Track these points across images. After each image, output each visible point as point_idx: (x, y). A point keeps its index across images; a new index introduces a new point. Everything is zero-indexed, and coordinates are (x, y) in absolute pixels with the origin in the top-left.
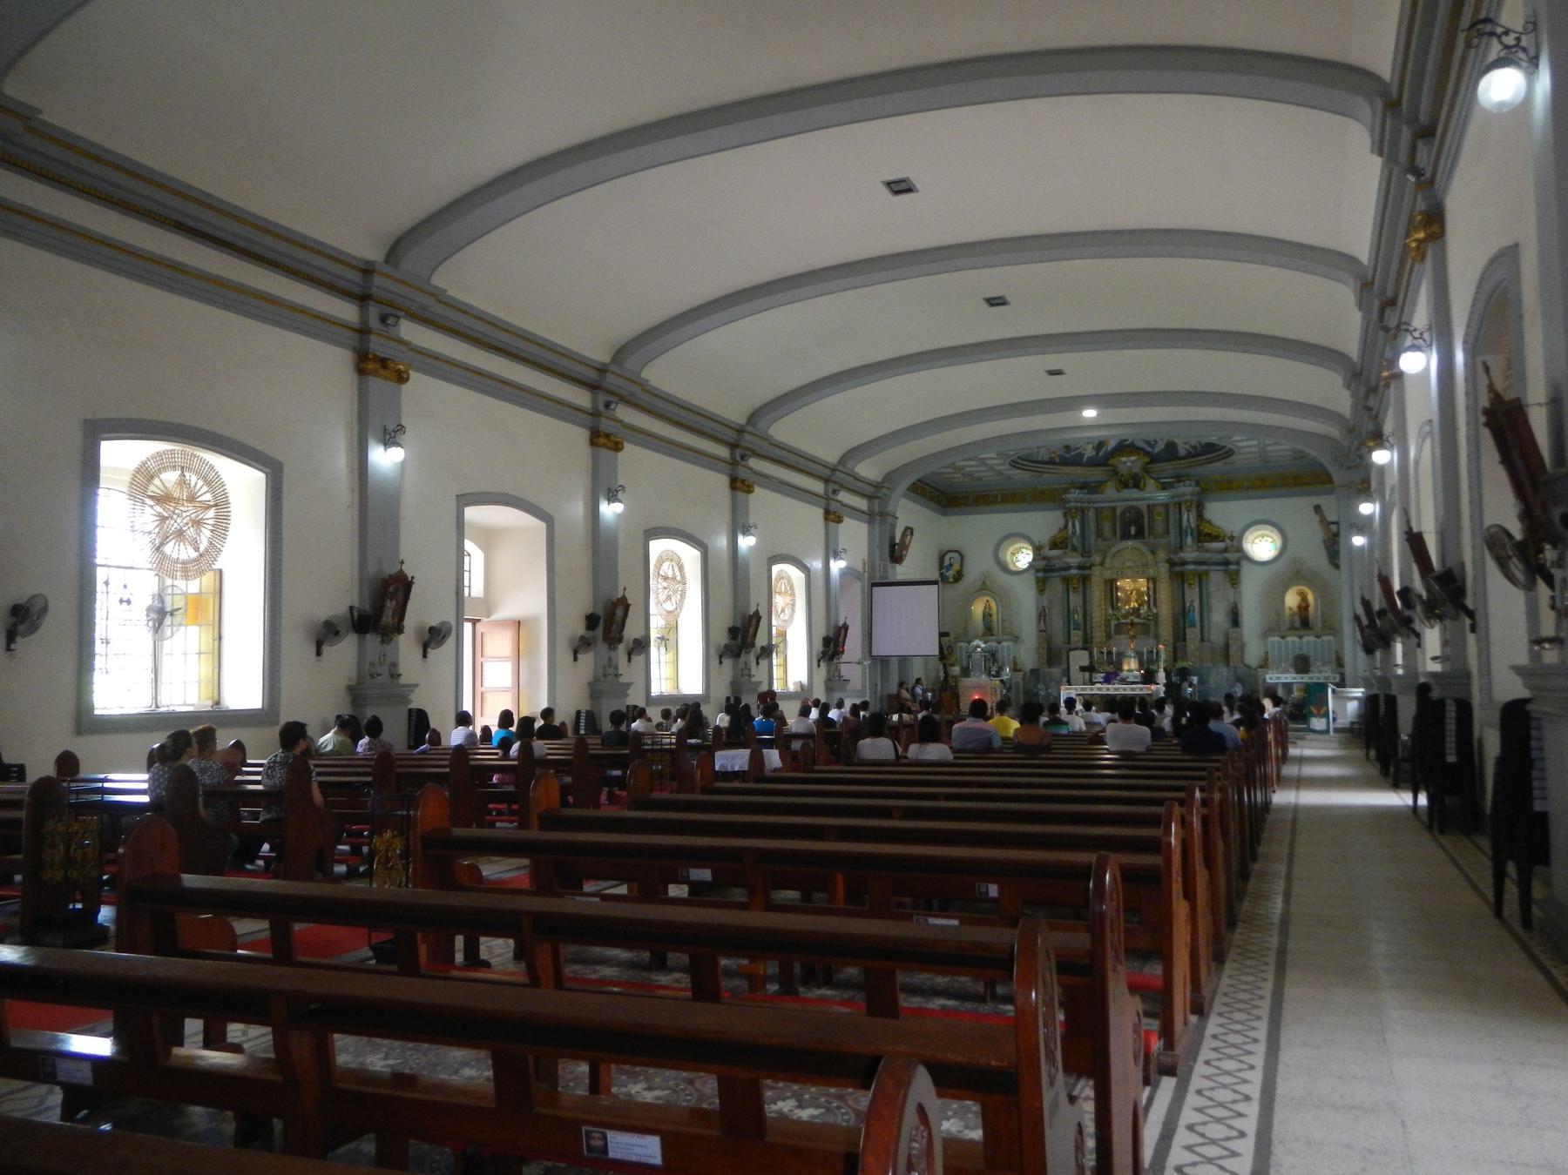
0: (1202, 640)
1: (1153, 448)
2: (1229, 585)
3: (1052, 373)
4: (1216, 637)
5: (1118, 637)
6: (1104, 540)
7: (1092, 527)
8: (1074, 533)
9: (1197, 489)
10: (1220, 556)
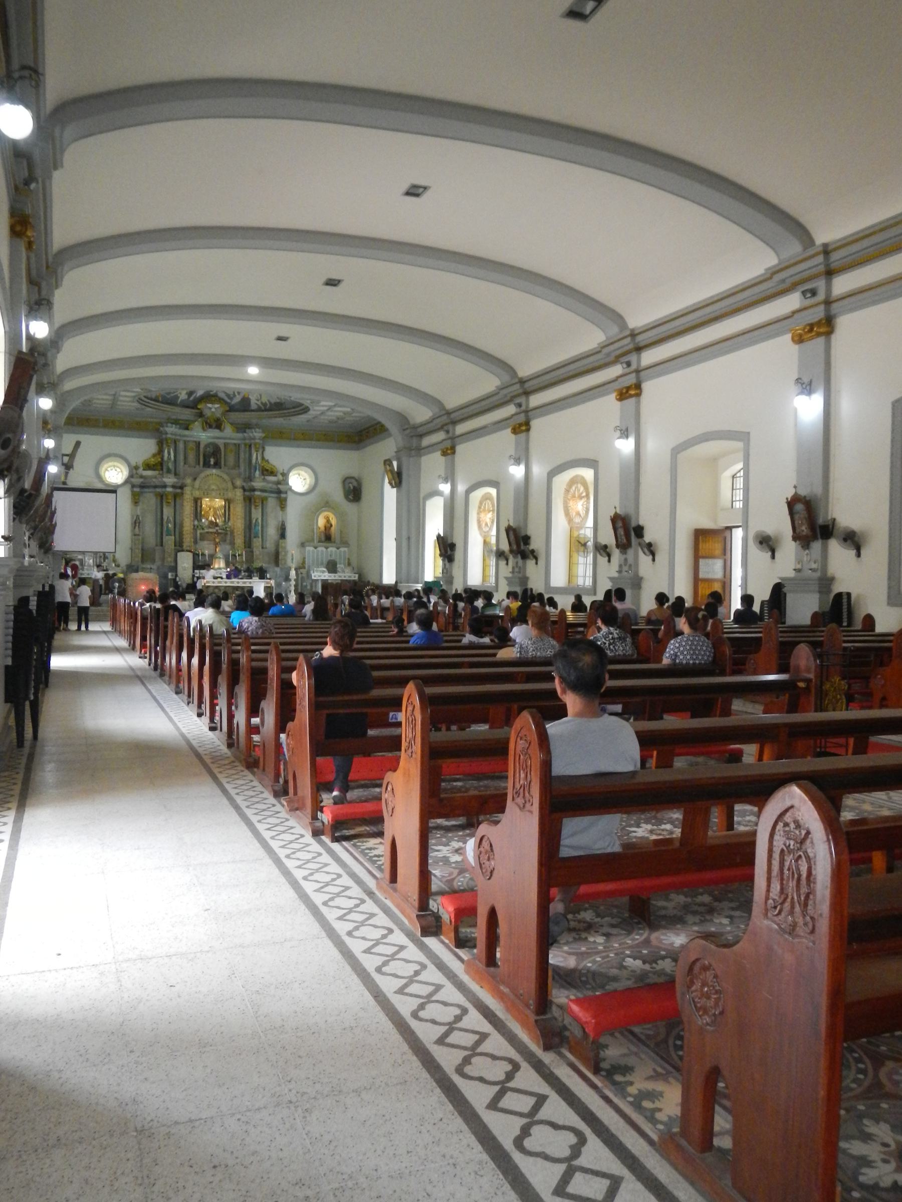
0: (262, 548)
2: (279, 508)
3: (280, 339)
4: (270, 545)
6: (189, 466)
8: (169, 458)
9: (264, 435)
10: (275, 486)
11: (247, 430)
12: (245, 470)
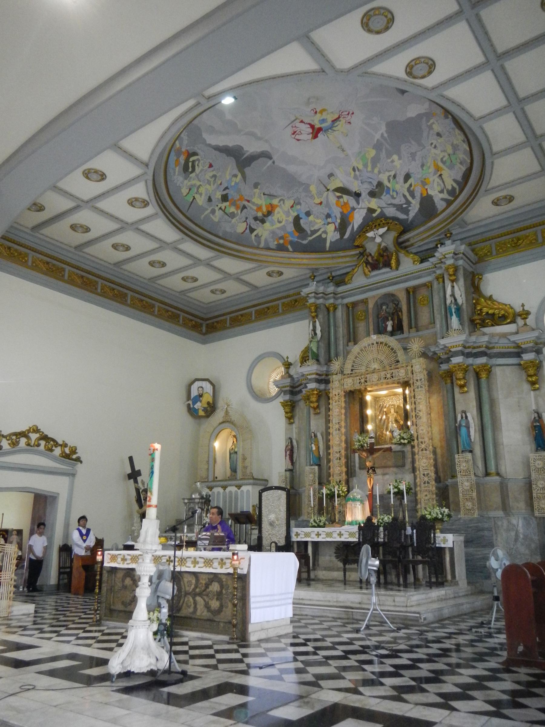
1: (408, 215)
2: (526, 386)
5: (362, 471)
7: (341, 331)
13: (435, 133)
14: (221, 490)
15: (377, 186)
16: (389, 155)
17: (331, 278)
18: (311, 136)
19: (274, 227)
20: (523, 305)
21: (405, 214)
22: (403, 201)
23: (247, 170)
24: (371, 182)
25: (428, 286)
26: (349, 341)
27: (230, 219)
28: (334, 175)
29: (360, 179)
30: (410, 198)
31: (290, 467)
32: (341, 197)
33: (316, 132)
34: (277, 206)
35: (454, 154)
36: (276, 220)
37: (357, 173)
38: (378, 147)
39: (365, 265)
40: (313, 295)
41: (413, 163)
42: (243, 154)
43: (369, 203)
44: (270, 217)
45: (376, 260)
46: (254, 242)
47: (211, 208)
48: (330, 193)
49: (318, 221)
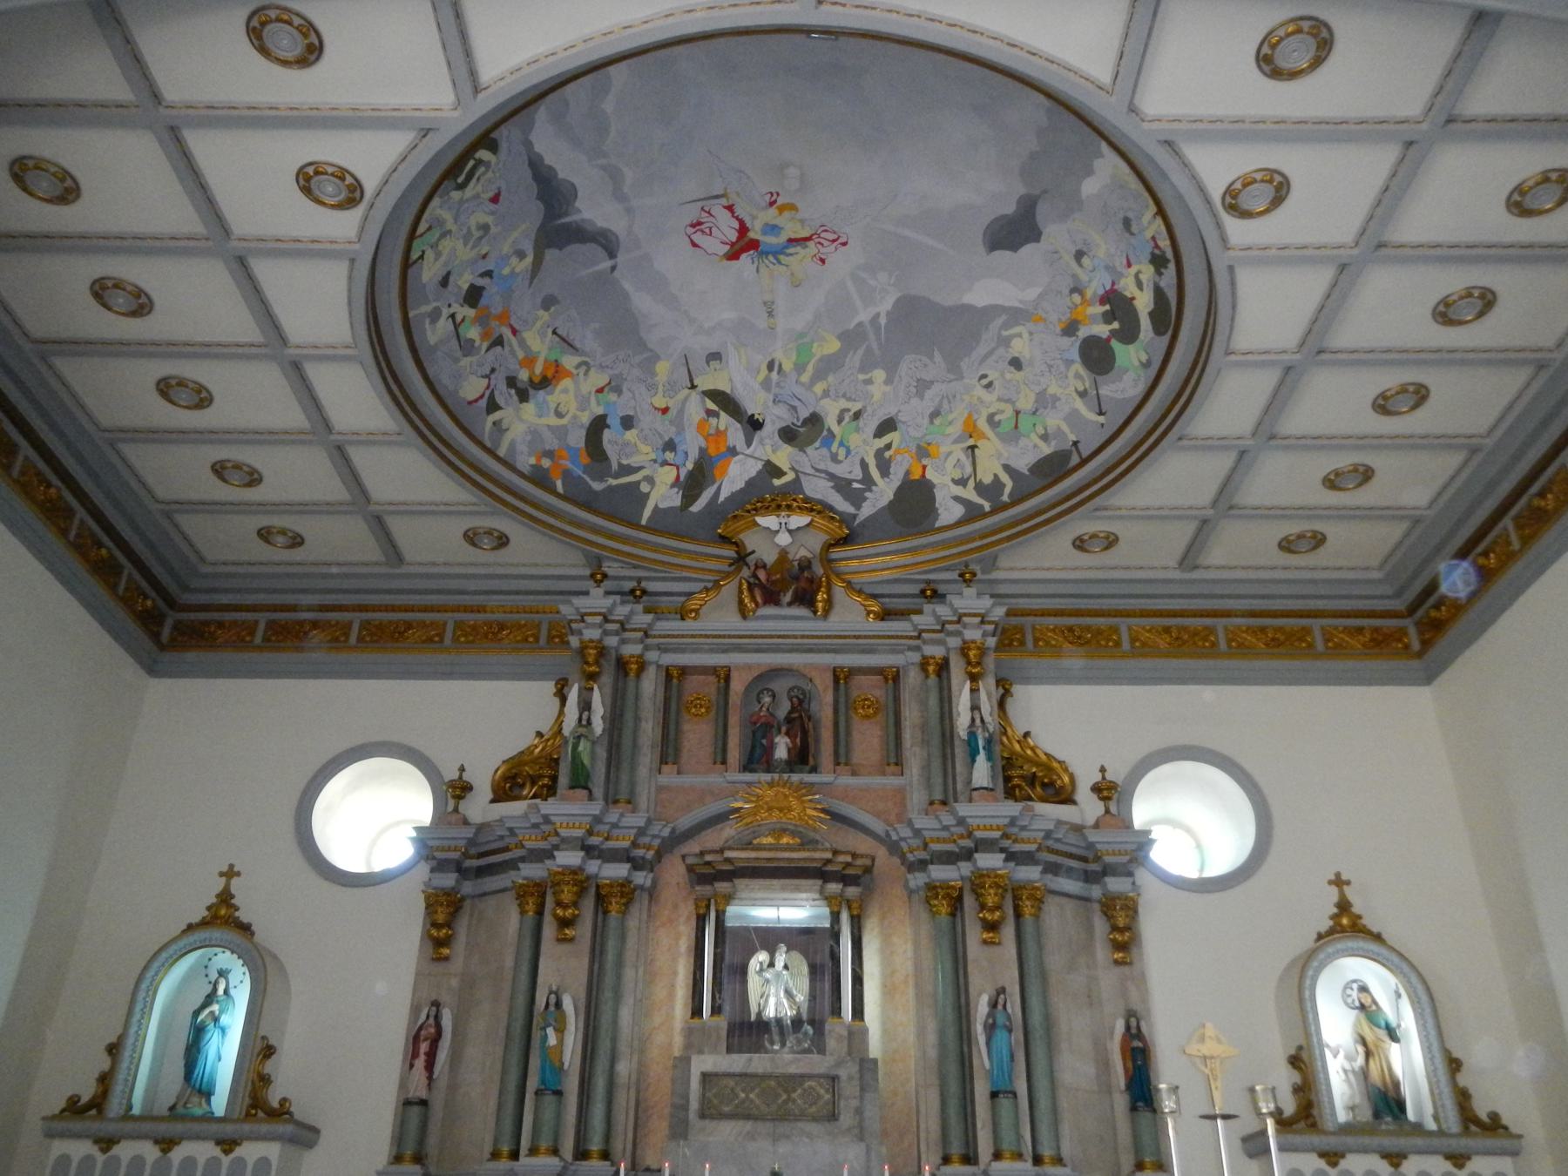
1: (858, 507)
2: (1102, 953)
5: (707, 1121)
7: (649, 730)
8: (584, 723)
11: (927, 608)
12: (926, 768)
13: (1009, 357)
14: (150, 1152)
15: (806, 422)
16: (863, 369)
17: (638, 593)
18: (728, 247)
19: (544, 421)
20: (1103, 770)
21: (853, 504)
22: (858, 473)
23: (551, 255)
24: (794, 408)
25: (893, 677)
26: (664, 760)
27: (459, 354)
28: (721, 360)
29: (775, 390)
30: (875, 473)
31: (423, 1094)
32: (716, 415)
33: (743, 245)
34: (569, 374)
35: (1034, 413)
36: (553, 406)
37: (774, 375)
38: (851, 338)
39: (745, 586)
40: (599, 619)
41: (915, 401)
42: (566, 214)
43: (774, 451)
44: (541, 393)
45: (774, 583)
46: (486, 436)
47: (435, 304)
48: (695, 397)
49: (644, 448)
